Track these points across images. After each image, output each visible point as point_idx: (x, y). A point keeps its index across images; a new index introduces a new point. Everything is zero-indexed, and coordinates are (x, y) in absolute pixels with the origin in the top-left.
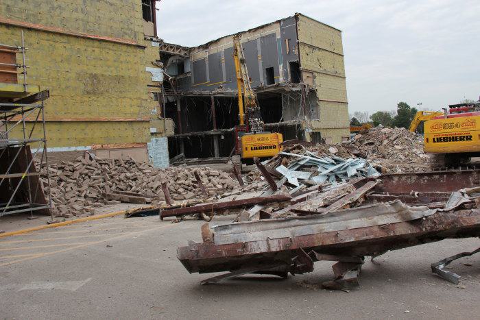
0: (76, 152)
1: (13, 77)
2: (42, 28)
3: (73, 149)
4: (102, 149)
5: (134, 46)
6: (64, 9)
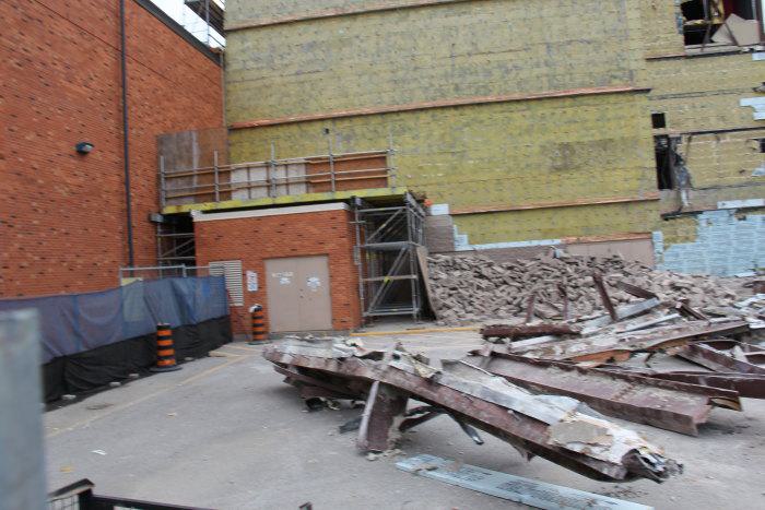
0: (539, 247)
1: (383, 182)
2: (494, 99)
3: (535, 243)
4: (579, 243)
5: (630, 92)
6: (521, 69)
